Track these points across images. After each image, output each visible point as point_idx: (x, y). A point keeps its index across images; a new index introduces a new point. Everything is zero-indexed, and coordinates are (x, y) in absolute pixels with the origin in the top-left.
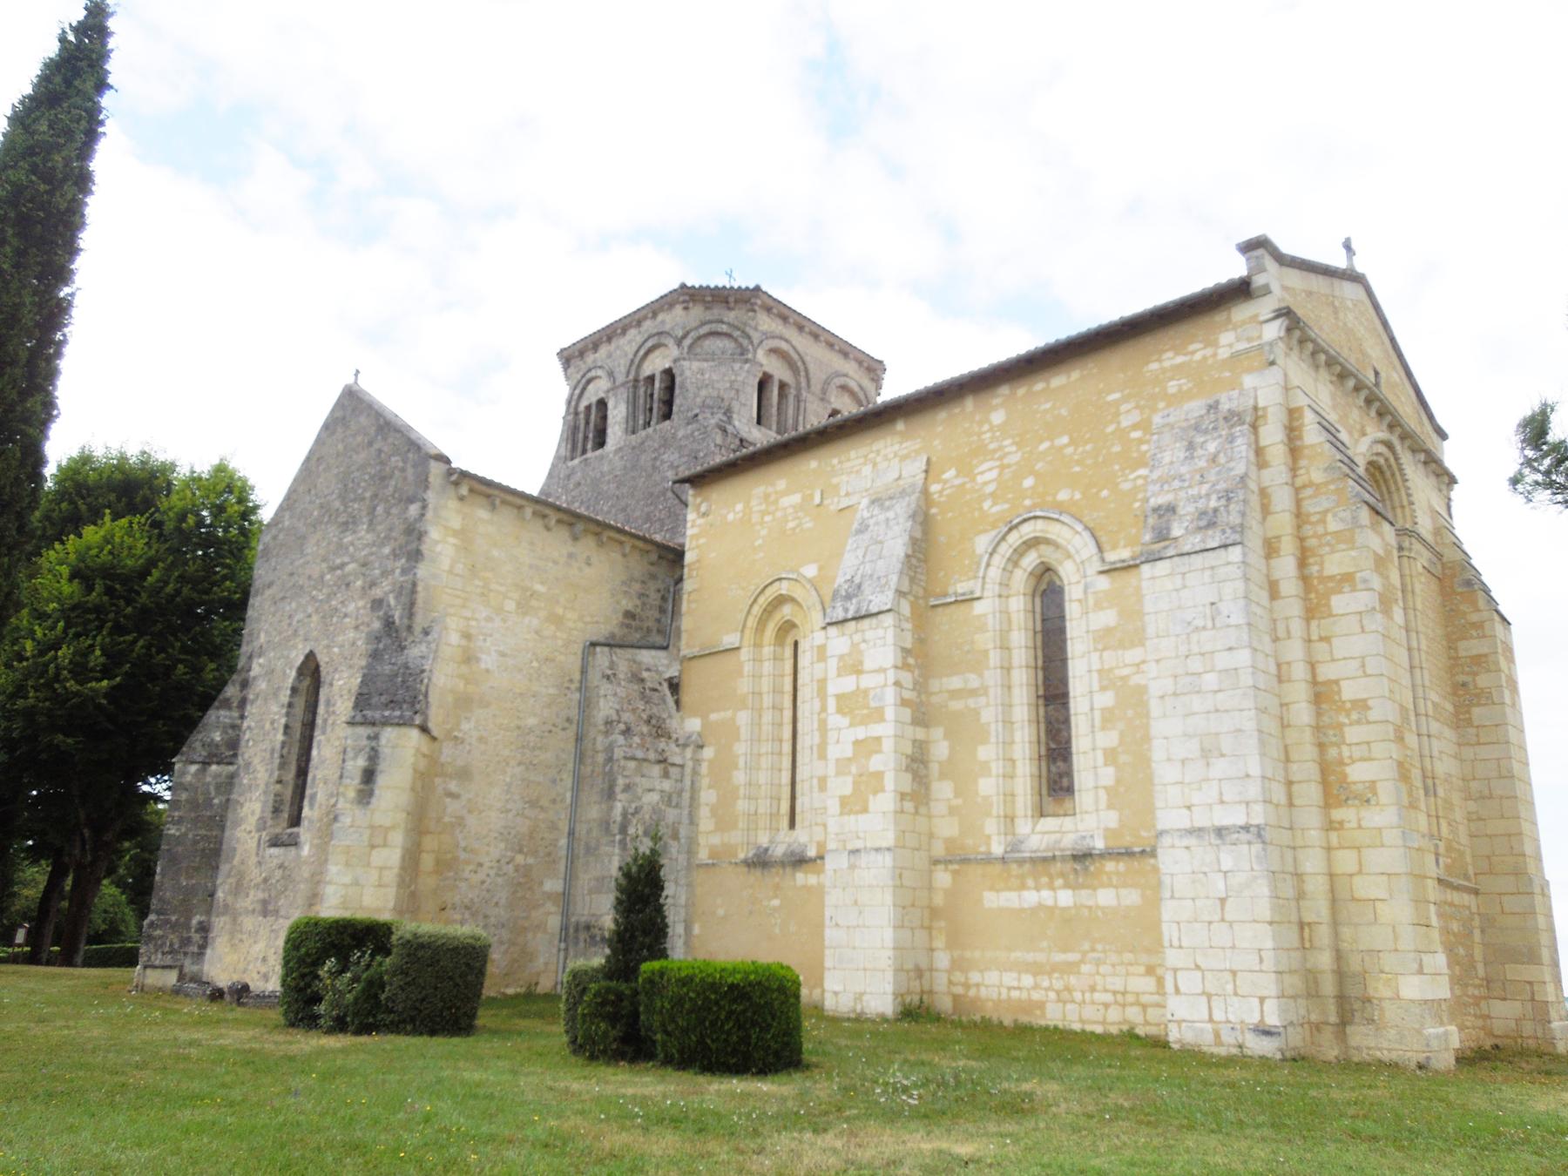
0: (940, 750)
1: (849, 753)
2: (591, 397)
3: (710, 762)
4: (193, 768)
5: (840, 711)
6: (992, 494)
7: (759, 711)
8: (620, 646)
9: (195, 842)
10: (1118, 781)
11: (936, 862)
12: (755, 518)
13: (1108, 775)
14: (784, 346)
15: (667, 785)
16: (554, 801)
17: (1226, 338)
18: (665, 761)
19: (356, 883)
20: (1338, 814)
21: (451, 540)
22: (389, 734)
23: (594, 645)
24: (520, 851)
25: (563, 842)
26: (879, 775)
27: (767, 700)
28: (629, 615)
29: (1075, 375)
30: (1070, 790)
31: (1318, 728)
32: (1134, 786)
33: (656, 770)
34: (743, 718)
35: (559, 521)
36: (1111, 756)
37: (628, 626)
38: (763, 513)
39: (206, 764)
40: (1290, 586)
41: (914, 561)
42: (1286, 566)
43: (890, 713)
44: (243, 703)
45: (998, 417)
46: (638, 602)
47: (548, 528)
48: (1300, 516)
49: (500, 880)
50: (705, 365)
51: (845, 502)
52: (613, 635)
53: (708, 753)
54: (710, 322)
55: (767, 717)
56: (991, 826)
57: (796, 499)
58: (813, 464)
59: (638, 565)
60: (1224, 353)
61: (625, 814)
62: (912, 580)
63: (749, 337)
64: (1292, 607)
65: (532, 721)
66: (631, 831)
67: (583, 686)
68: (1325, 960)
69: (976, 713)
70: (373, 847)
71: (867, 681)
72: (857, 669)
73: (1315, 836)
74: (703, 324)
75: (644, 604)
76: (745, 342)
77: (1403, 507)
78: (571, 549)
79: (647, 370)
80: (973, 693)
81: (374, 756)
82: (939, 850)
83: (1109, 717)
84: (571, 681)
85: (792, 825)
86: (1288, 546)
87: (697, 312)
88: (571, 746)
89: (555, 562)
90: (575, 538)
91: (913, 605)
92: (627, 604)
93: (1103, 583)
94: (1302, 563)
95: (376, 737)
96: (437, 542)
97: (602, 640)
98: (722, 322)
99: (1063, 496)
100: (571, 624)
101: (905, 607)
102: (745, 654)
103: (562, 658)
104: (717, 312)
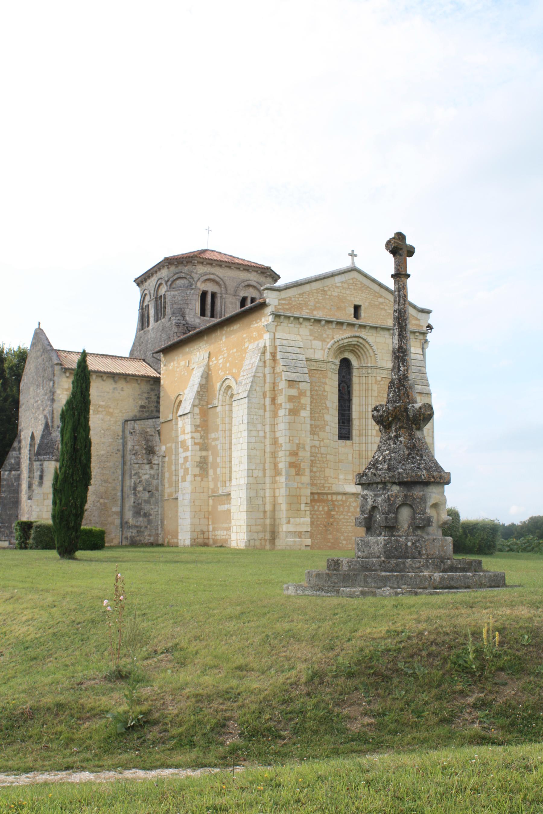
2: (146, 303)
4: (7, 473)
8: (138, 420)
9: (10, 499)
11: (209, 497)
14: (212, 277)
15: (152, 472)
16: (114, 480)
18: (151, 463)
19: (40, 511)
21: (65, 393)
22: (46, 463)
23: (126, 421)
24: (102, 498)
25: (119, 494)
28: (142, 407)
29: (238, 325)
33: (147, 467)
35: (107, 377)
37: (142, 411)
39: (10, 471)
41: (201, 393)
44: (20, 448)
46: (147, 401)
47: (103, 380)
49: (94, 508)
50: (176, 293)
52: (136, 416)
53: (166, 459)
54: (177, 273)
58: (187, 350)
59: (145, 387)
61: (135, 483)
62: (200, 400)
63: (193, 278)
65: (102, 452)
66: (138, 489)
67: (124, 438)
68: (268, 522)
69: (217, 446)
70: (44, 499)
74: (175, 274)
75: (149, 401)
77: (371, 357)
78: (115, 386)
81: (42, 471)
84: (118, 436)
87: (173, 269)
88: (120, 460)
89: (108, 393)
90: (115, 382)
91: (200, 409)
92: (141, 403)
95: (41, 465)
96: (59, 394)
97: (131, 418)
98: (182, 272)
100: (117, 415)
101: (197, 410)
103: (114, 428)
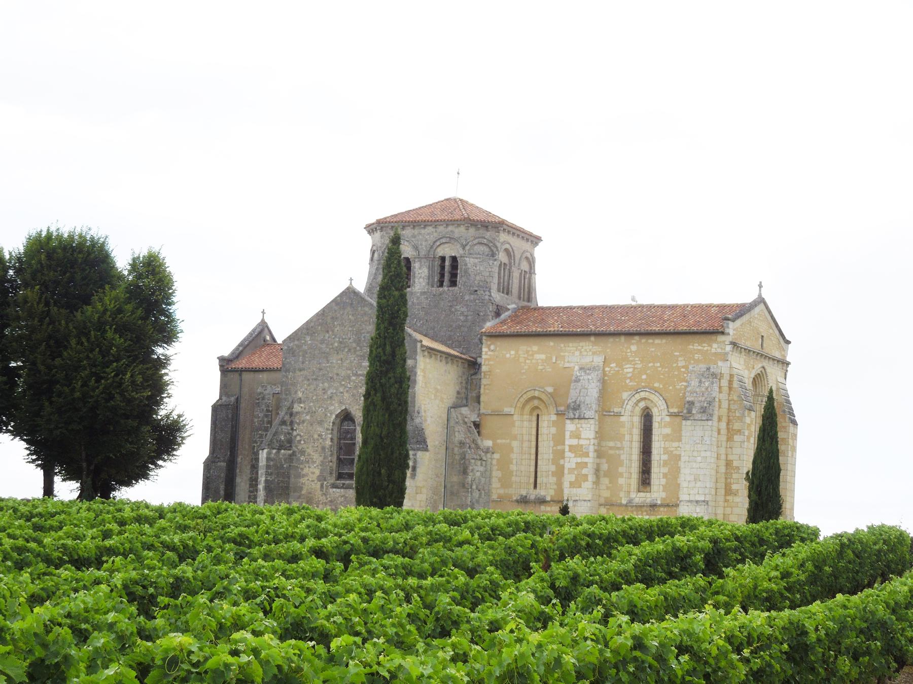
0: (605, 467)
1: (574, 466)
3: (498, 460)
4: (274, 451)
5: (570, 451)
6: (630, 378)
7: (522, 442)
10: (667, 483)
11: (601, 505)
12: (521, 360)
13: (663, 481)
17: (715, 345)
20: (728, 498)
26: (586, 476)
27: (526, 438)
30: (649, 484)
31: (726, 473)
32: (673, 485)
33: (479, 463)
34: (515, 444)
36: (665, 475)
38: (526, 359)
39: (279, 450)
40: (724, 432)
42: (723, 425)
43: (591, 454)
45: (634, 348)
48: (729, 409)
50: (476, 261)
51: (567, 365)
53: (496, 456)
55: (526, 444)
56: (622, 494)
57: (543, 357)
58: (552, 344)
60: (713, 351)
63: (496, 247)
64: (724, 438)
69: (619, 455)
71: (582, 442)
72: (578, 437)
73: (721, 503)
74: (475, 238)
76: (495, 250)
79: (441, 252)
80: (618, 448)
82: (602, 501)
83: (665, 463)
85: (535, 487)
86: (725, 419)
93: (668, 419)
94: (728, 424)
99: (656, 385)
102: (515, 417)
104: (482, 231)
